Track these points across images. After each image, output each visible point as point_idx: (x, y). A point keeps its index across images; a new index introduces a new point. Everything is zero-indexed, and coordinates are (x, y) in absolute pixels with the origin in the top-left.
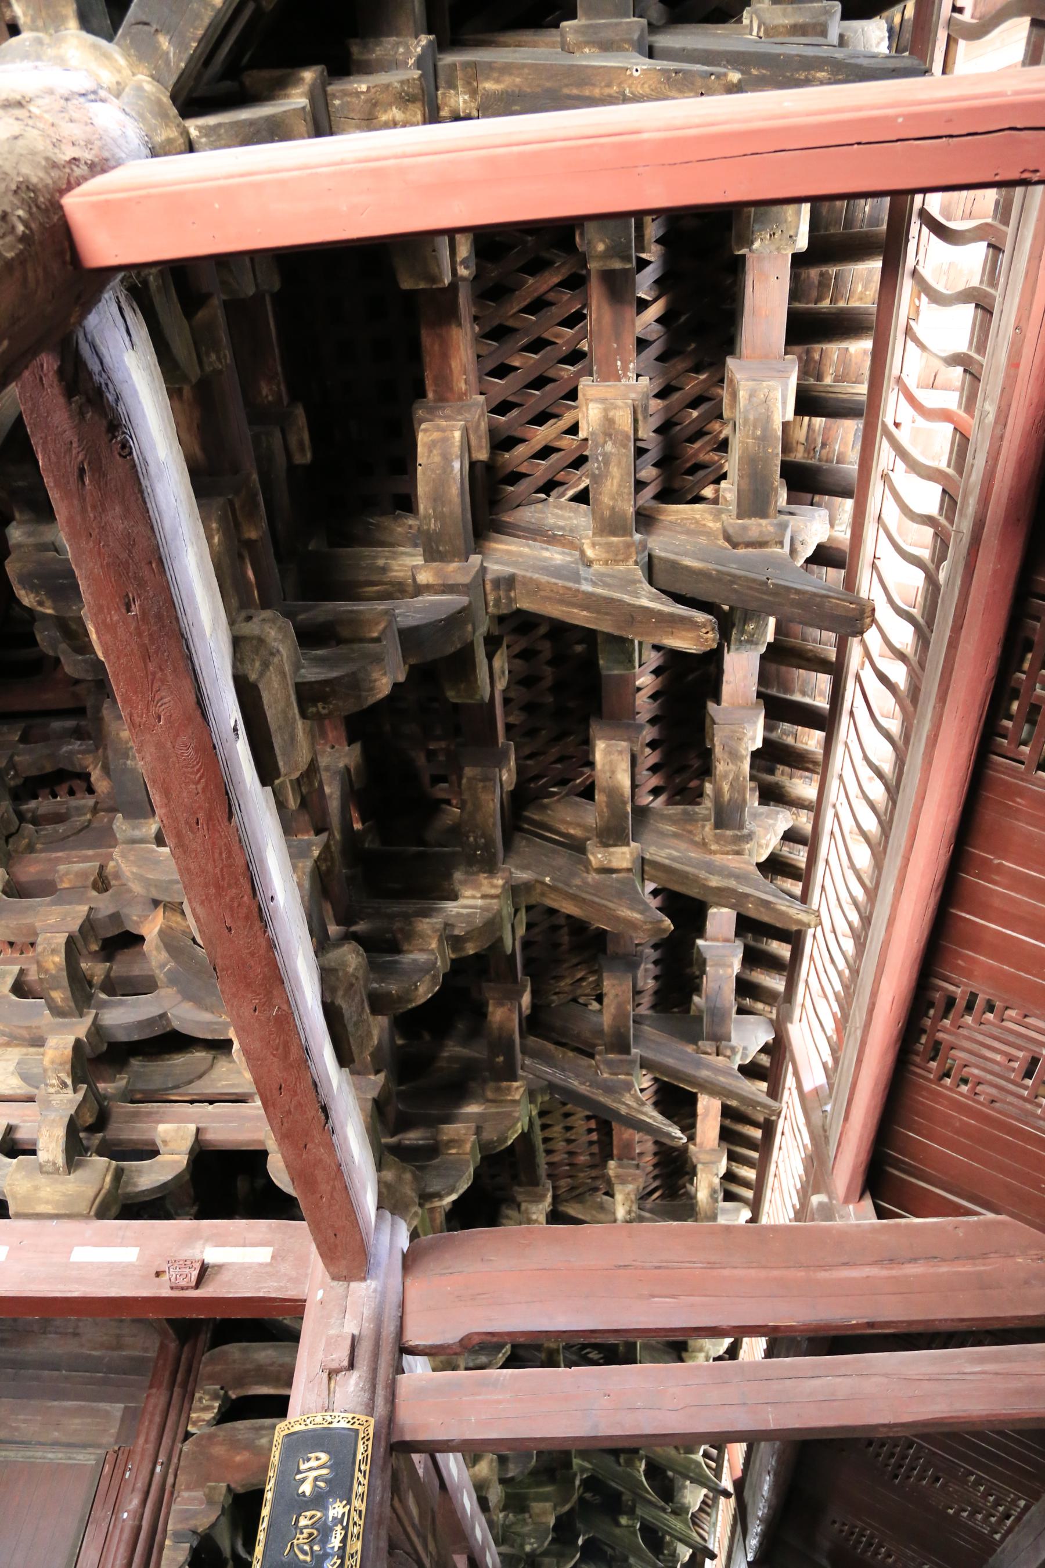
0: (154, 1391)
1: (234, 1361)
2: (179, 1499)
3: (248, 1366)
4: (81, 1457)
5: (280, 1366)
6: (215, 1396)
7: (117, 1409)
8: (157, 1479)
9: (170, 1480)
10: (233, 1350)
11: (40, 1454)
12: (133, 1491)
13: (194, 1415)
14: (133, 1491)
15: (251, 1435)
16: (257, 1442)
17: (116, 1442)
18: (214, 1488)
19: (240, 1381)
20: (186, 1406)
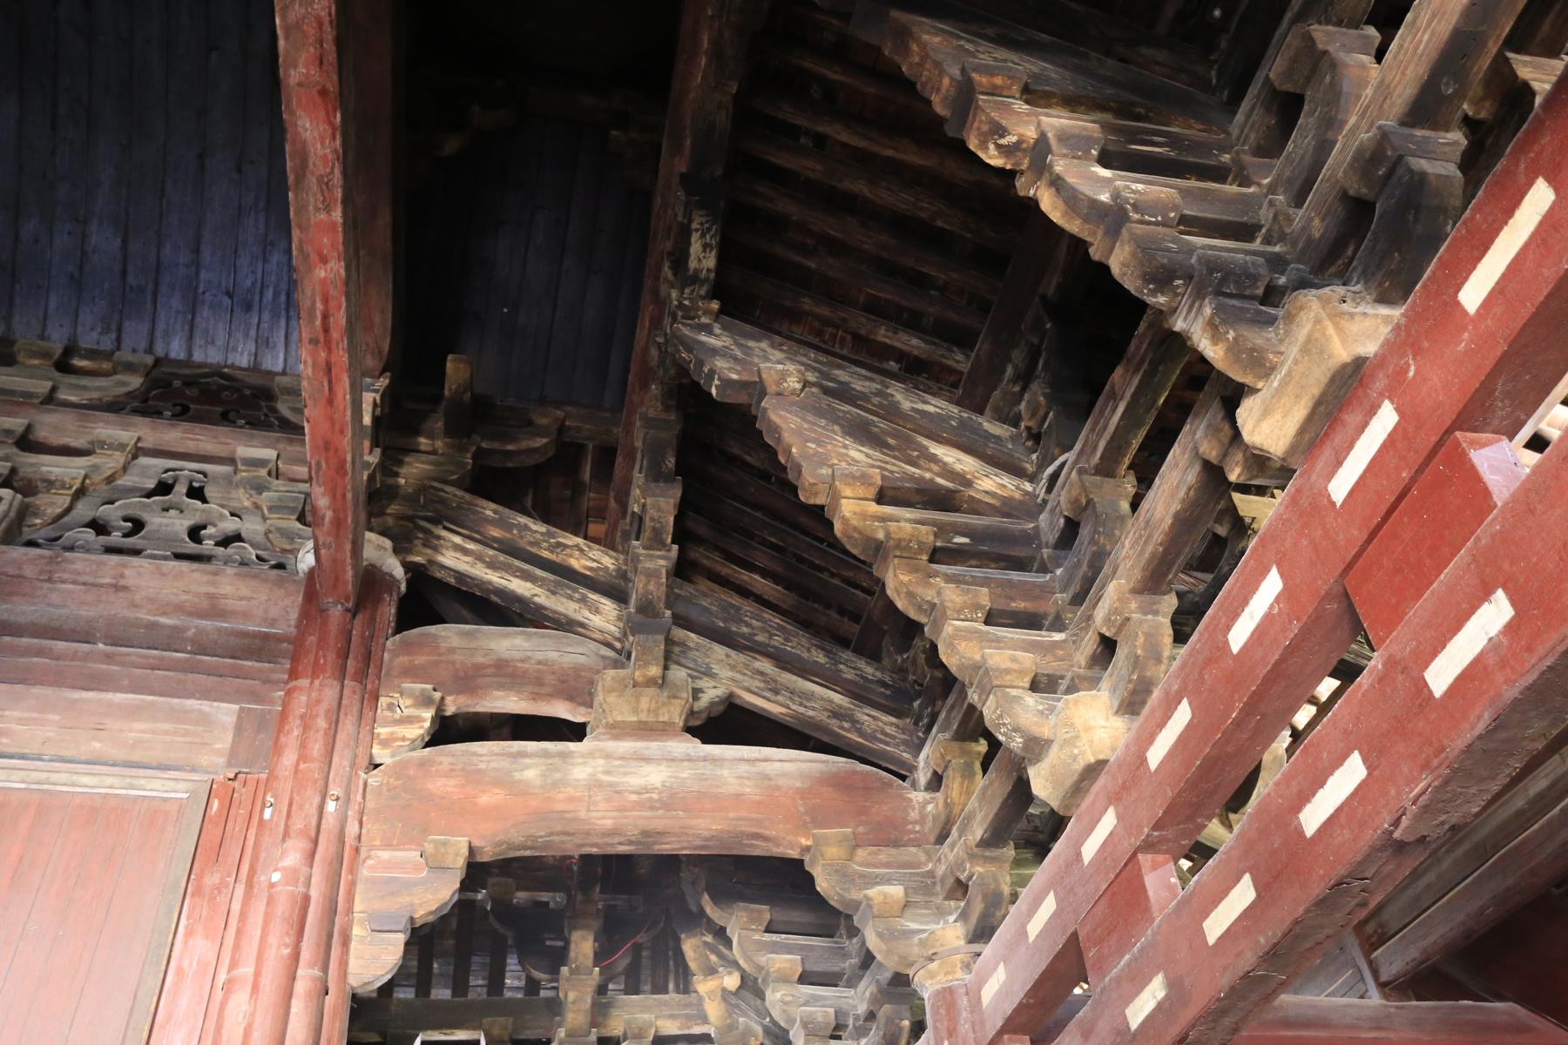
0: (304, 682)
1: (452, 650)
2: (370, 862)
3: (479, 659)
4: (157, 784)
5: (539, 663)
6: (425, 701)
7: (226, 713)
8: (329, 822)
9: (352, 829)
10: (449, 635)
11: (63, 777)
12: (286, 835)
13: (382, 731)
14: (286, 835)
15: (504, 764)
16: (517, 775)
17: (229, 765)
18: (445, 844)
19: (467, 680)
20: (368, 714)
